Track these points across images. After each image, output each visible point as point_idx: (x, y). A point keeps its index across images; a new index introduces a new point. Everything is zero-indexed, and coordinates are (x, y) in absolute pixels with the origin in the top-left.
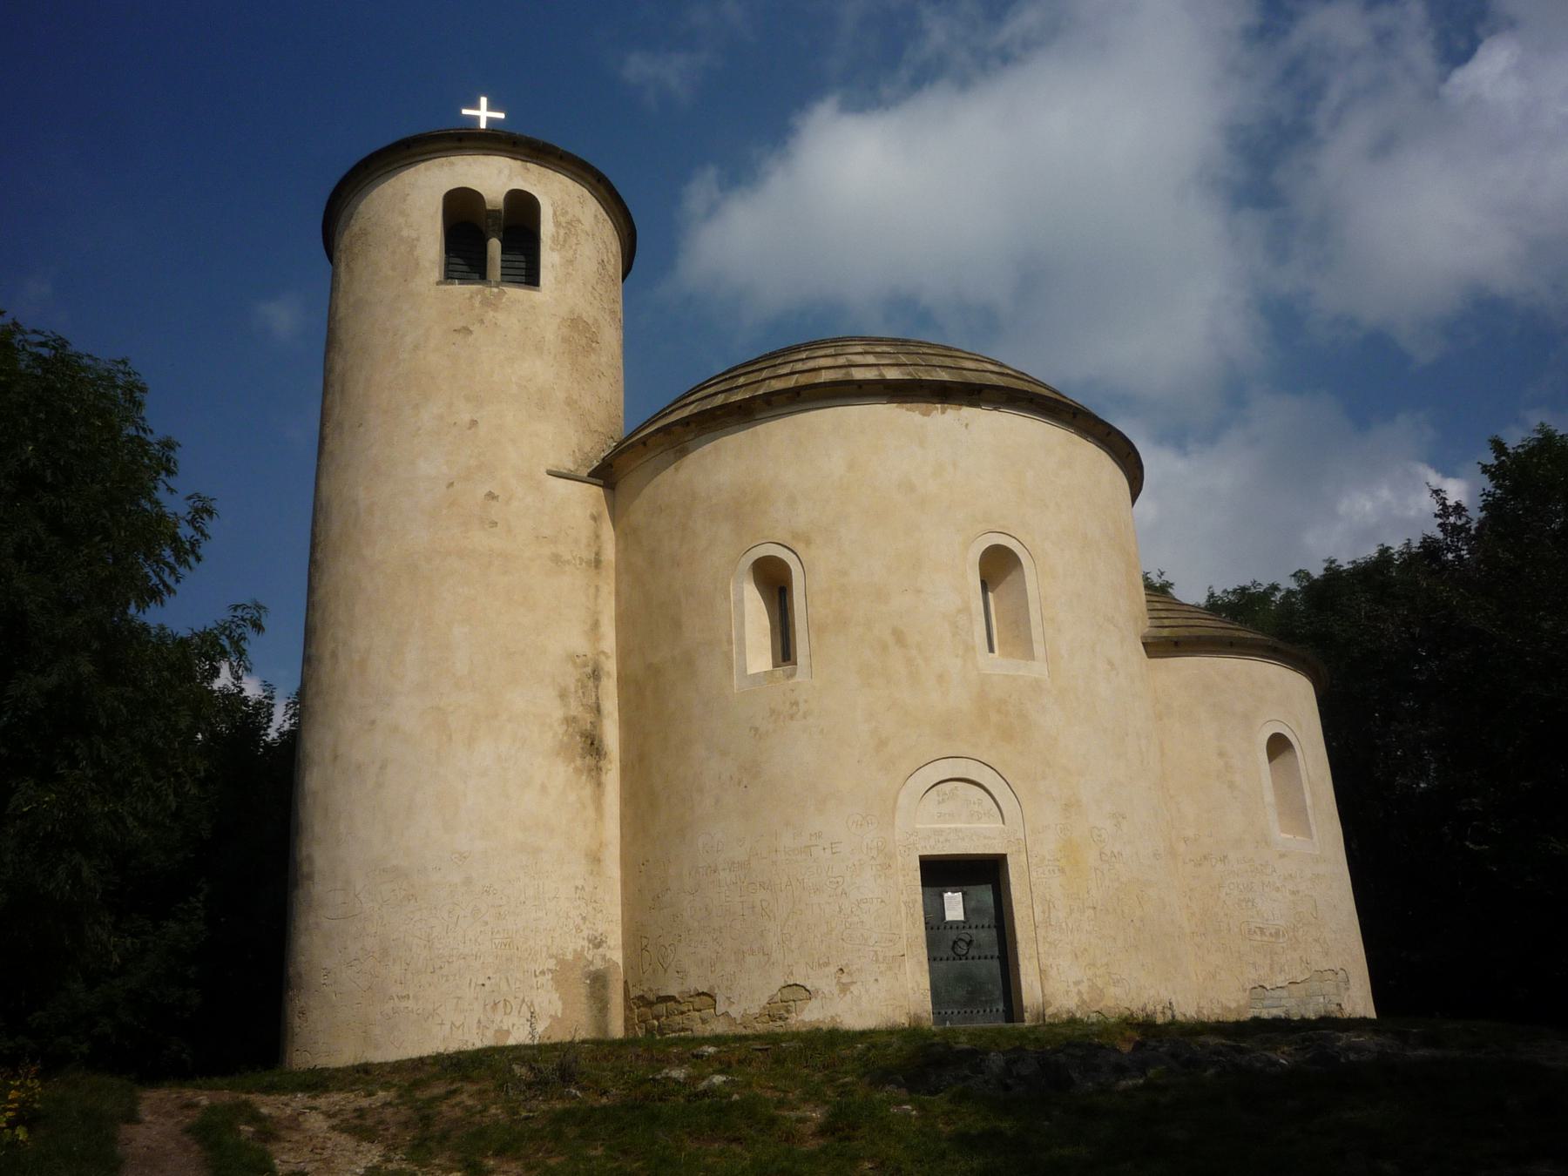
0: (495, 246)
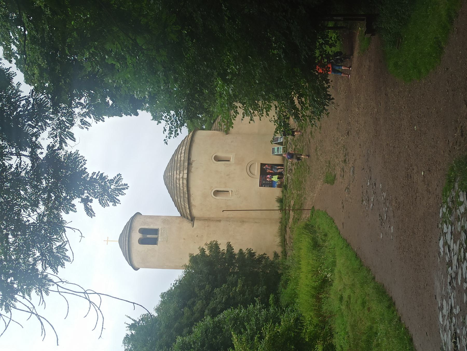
0: (149, 236)
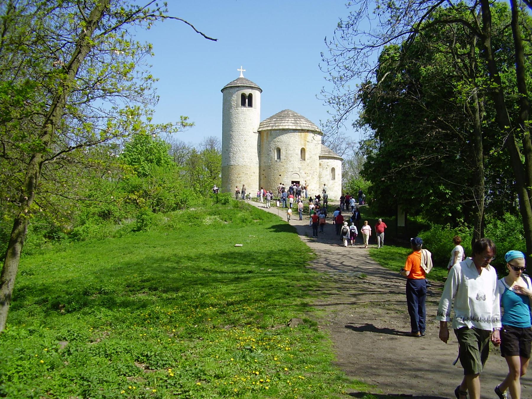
0: (247, 100)
